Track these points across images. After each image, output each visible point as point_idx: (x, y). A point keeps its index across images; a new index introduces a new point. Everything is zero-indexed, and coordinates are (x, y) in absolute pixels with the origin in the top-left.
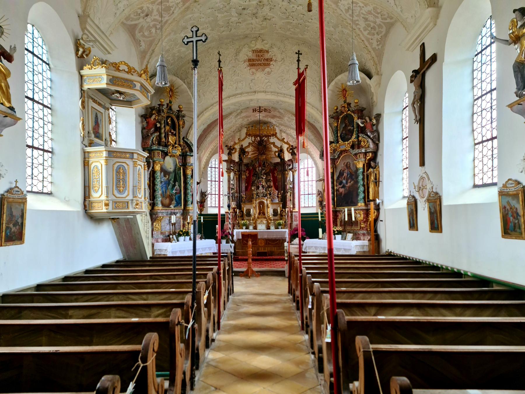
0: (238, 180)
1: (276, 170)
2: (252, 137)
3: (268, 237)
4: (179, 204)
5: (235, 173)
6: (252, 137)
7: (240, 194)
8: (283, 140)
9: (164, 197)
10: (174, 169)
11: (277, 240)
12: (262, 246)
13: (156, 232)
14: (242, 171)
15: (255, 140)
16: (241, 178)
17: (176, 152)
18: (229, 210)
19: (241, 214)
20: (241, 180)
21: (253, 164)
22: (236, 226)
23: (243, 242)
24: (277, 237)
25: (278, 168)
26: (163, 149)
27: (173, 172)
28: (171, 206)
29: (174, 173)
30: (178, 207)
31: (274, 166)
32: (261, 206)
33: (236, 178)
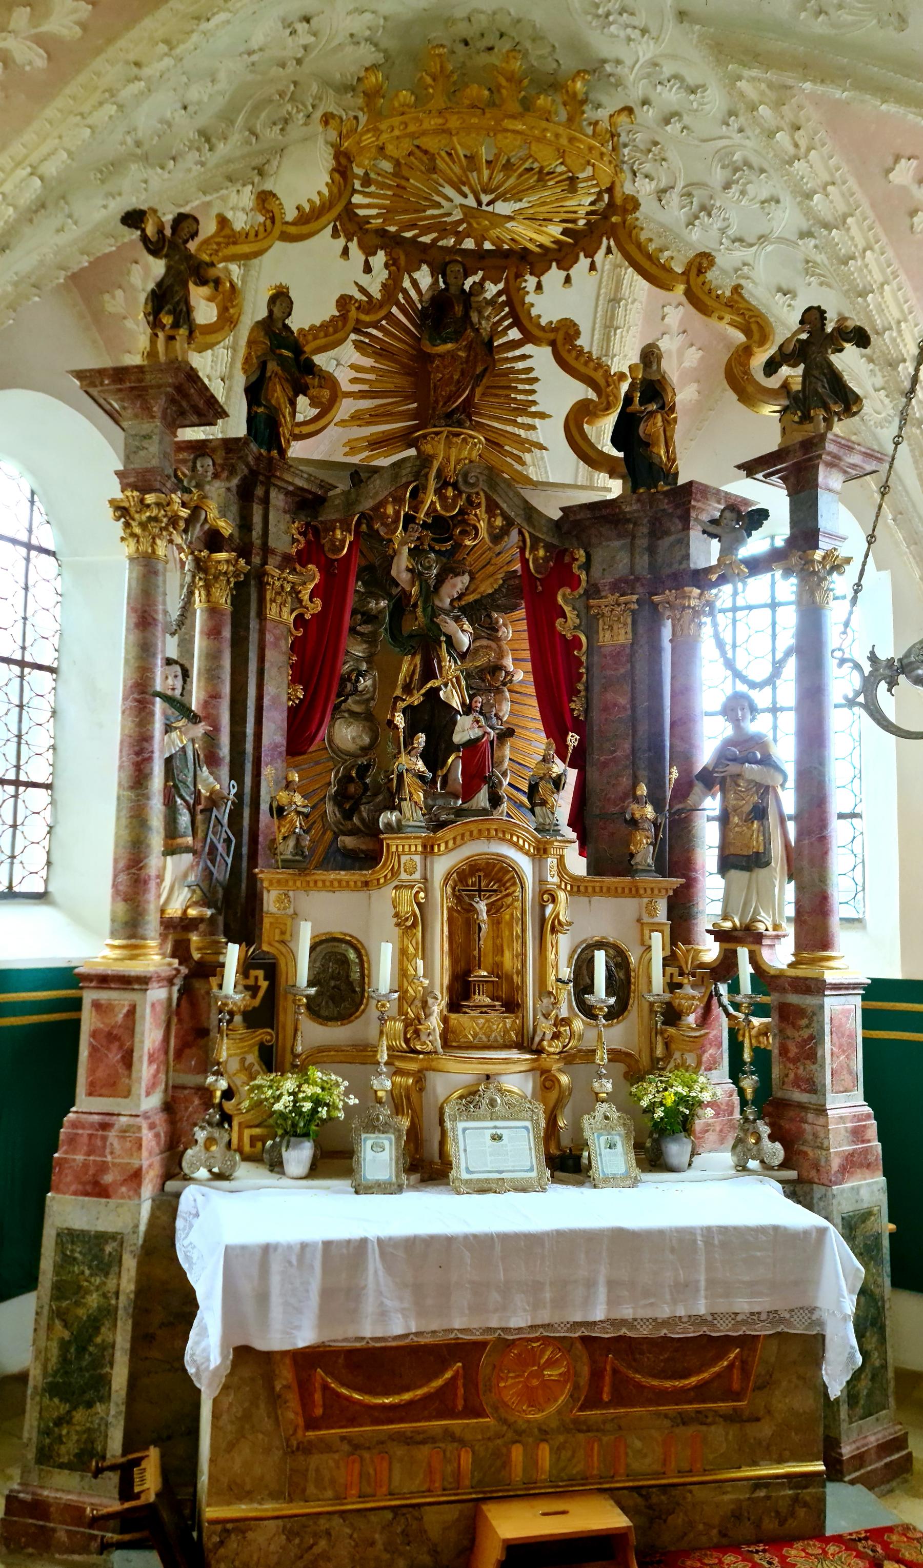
0: (227, 633)
1: (574, 583)
2: (369, 252)
3: (627, 1312)
5: (200, 566)
6: (369, 252)
7: (236, 773)
8: (700, 272)
11: (727, 1342)
12: (544, 1434)
14: (266, 550)
15: (391, 288)
16: (254, 624)
18: (134, 949)
19: (253, 989)
20: (254, 637)
21: (367, 505)
22: (201, 1135)
23: (304, 1389)
24: (722, 1306)
25: (587, 566)
31: (548, 547)
32: (482, 907)
33: (213, 611)
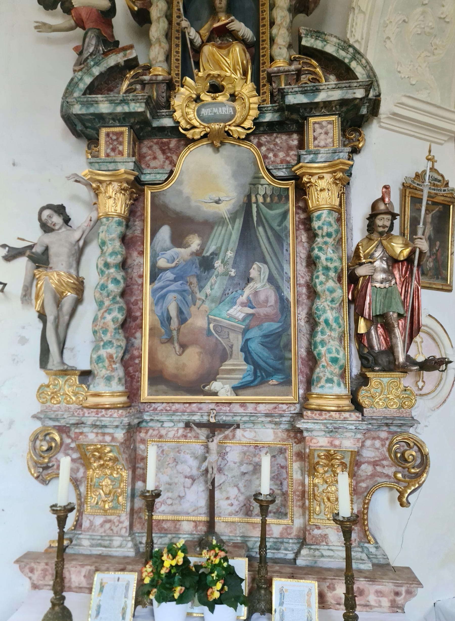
4: (269, 375)
9: (170, 340)
10: (243, 199)
13: (99, 520)
17: (225, 111)
26: (119, 109)
27: (233, 219)
28: (215, 386)
29: (239, 223)
30: (264, 388)
